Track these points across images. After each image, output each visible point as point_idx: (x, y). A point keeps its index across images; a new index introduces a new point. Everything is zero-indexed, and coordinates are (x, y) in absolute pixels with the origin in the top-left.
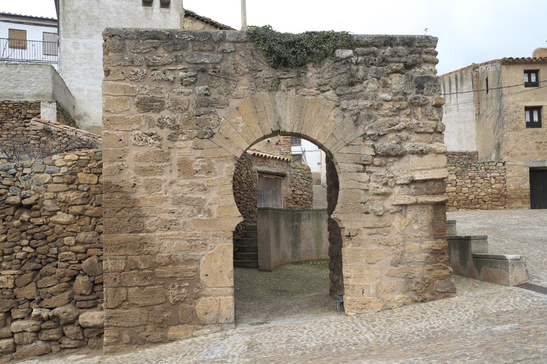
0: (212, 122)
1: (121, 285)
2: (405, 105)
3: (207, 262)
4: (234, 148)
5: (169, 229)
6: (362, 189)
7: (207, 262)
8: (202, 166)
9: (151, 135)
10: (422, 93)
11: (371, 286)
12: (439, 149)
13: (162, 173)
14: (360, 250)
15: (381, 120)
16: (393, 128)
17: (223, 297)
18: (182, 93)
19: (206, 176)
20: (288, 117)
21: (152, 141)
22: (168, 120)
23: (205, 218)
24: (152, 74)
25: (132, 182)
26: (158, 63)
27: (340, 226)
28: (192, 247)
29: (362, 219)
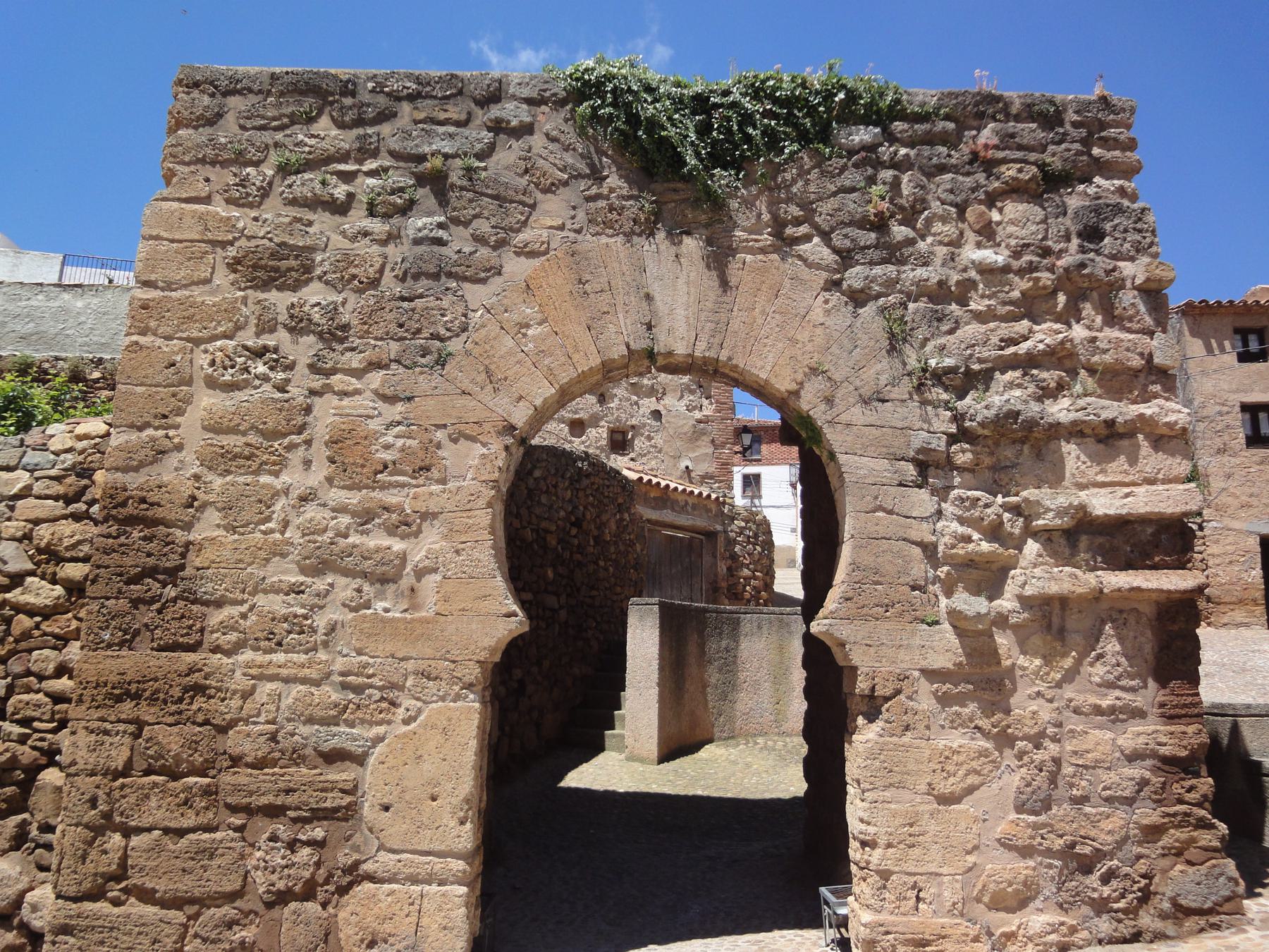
0: (445, 319)
1: (106, 824)
2: (1049, 283)
3: (391, 761)
4: (506, 400)
5: (279, 644)
6: (913, 543)
7: (391, 761)
8: (402, 450)
9: (259, 353)
10: (1098, 252)
11: (946, 879)
12: (1167, 419)
13: (278, 466)
14: (906, 748)
15: (971, 330)
16: (1012, 350)
17: (434, 888)
18: (366, 234)
19: (414, 482)
20: (681, 312)
21: (261, 369)
22: (316, 309)
23: (398, 615)
24: (286, 183)
25: (187, 489)
26: (310, 153)
27: (842, 663)
28: (346, 707)
29: (917, 641)
